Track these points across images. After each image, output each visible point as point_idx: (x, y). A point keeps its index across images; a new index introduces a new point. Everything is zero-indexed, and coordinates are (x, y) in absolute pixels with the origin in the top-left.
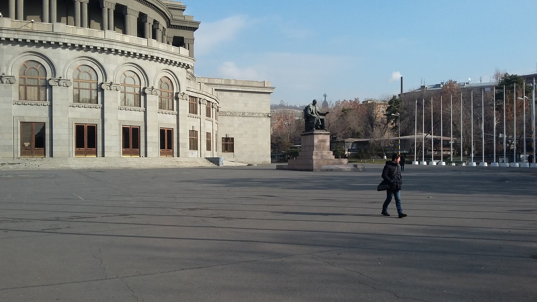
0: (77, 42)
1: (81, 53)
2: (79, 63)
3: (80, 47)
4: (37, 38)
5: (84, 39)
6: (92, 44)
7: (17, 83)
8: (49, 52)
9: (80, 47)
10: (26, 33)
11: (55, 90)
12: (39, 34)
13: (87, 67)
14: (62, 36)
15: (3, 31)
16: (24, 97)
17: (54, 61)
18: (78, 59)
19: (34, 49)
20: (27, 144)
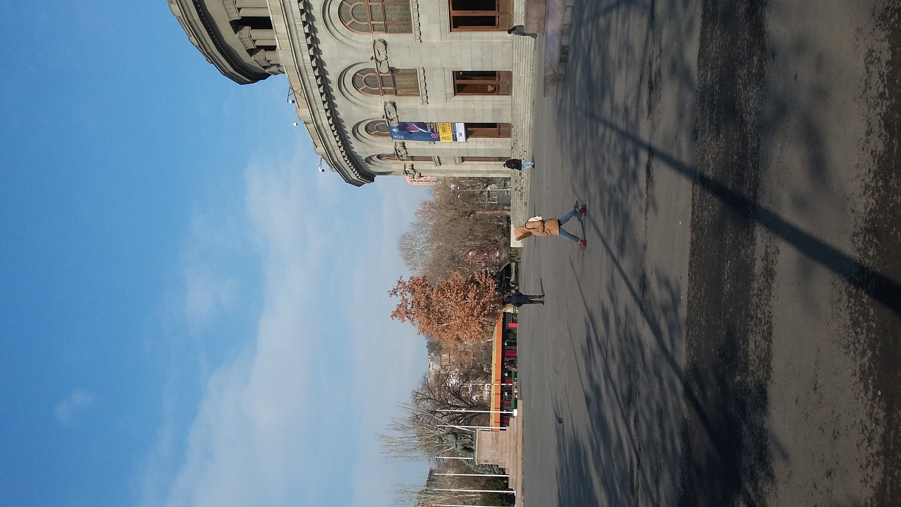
0: (304, 43)
1: (319, 24)
2: (339, 25)
3: (312, 34)
4: (316, 92)
5: (294, 32)
6: (297, 18)
7: (392, 98)
8: (332, 77)
9: (312, 34)
10: (313, 102)
11: (397, 65)
12: (309, 89)
13: (342, 10)
14: (302, 64)
15: (319, 123)
16: (413, 90)
17: (345, 64)
18: (331, 27)
19: (334, 86)
20: (490, 89)
